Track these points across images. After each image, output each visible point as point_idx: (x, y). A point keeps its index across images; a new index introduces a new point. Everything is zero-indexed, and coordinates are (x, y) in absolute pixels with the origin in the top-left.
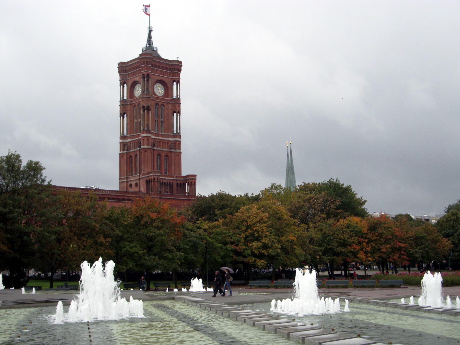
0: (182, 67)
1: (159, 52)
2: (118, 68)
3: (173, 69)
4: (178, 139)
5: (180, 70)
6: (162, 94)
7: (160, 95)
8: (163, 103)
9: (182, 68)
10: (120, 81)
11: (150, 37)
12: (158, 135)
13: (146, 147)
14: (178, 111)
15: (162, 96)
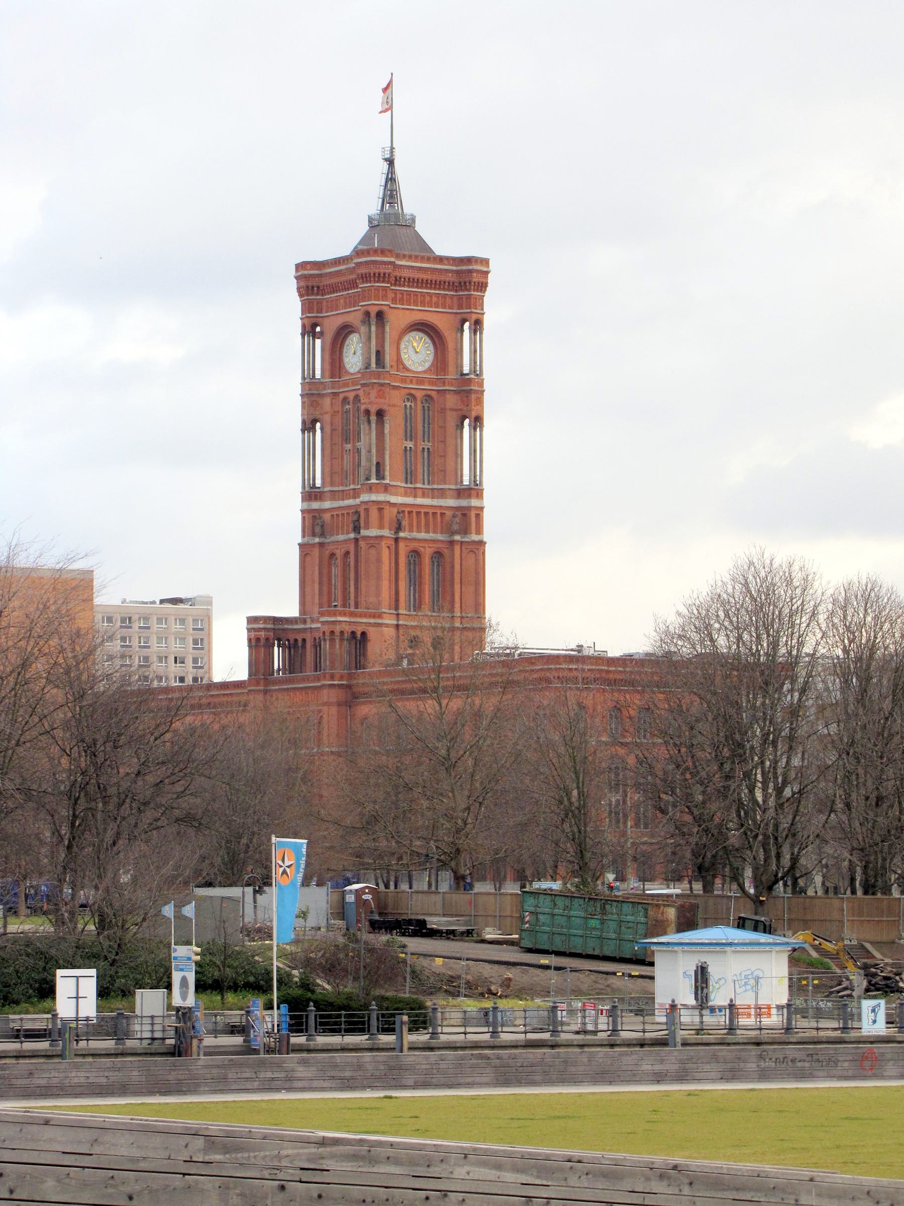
0: (489, 275)
1: (420, 228)
2: (296, 278)
3: (460, 283)
4: (474, 502)
5: (482, 286)
6: (427, 365)
7: (420, 369)
8: (429, 392)
9: (492, 280)
10: (301, 319)
11: (391, 179)
12: (414, 492)
13: (373, 532)
14: (474, 414)
15: (425, 372)
